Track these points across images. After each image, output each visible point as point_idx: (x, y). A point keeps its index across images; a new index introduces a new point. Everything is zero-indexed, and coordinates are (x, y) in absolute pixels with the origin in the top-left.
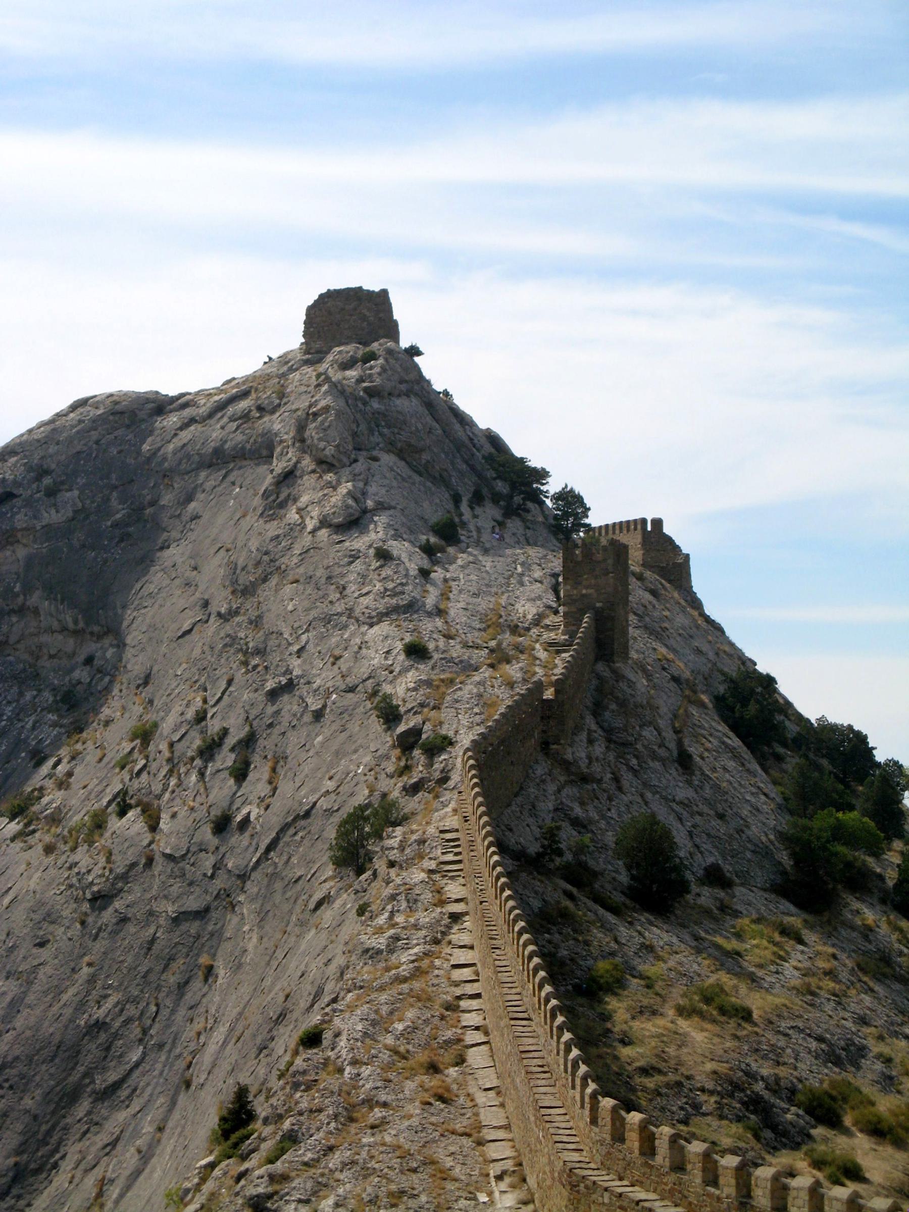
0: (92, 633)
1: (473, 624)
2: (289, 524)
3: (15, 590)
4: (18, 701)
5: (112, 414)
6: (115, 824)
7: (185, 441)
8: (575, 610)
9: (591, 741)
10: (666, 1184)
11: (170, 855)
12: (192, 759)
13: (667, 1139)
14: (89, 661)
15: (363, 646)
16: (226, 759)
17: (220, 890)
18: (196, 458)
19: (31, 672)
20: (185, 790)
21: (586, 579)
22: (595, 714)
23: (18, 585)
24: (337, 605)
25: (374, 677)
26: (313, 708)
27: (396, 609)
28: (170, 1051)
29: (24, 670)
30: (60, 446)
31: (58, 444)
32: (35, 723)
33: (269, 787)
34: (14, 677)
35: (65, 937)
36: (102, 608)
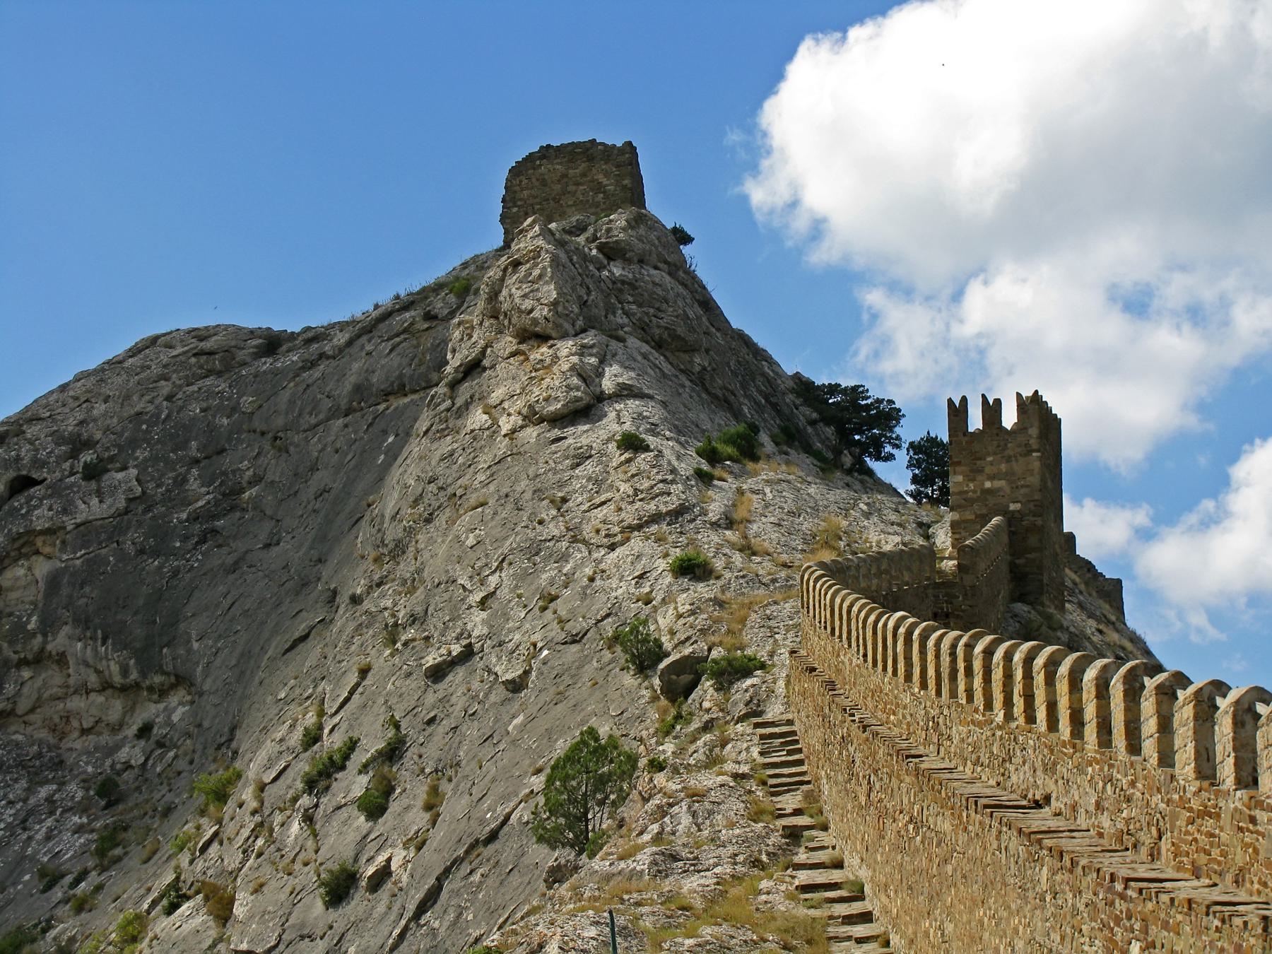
0: (151, 689)
1: (793, 544)
2: (472, 431)
3: (29, 627)
4: (25, 800)
5: (195, 355)
6: (162, 925)
7: (310, 381)
8: (973, 517)
12: (295, 799)
14: (145, 731)
16: (355, 784)
18: (328, 404)
23: (34, 618)
24: (550, 526)
26: (509, 676)
27: (656, 518)
29: (39, 755)
30: (110, 404)
31: (106, 401)
32: (50, 830)
33: (427, 816)
34: (21, 765)
36: (168, 645)
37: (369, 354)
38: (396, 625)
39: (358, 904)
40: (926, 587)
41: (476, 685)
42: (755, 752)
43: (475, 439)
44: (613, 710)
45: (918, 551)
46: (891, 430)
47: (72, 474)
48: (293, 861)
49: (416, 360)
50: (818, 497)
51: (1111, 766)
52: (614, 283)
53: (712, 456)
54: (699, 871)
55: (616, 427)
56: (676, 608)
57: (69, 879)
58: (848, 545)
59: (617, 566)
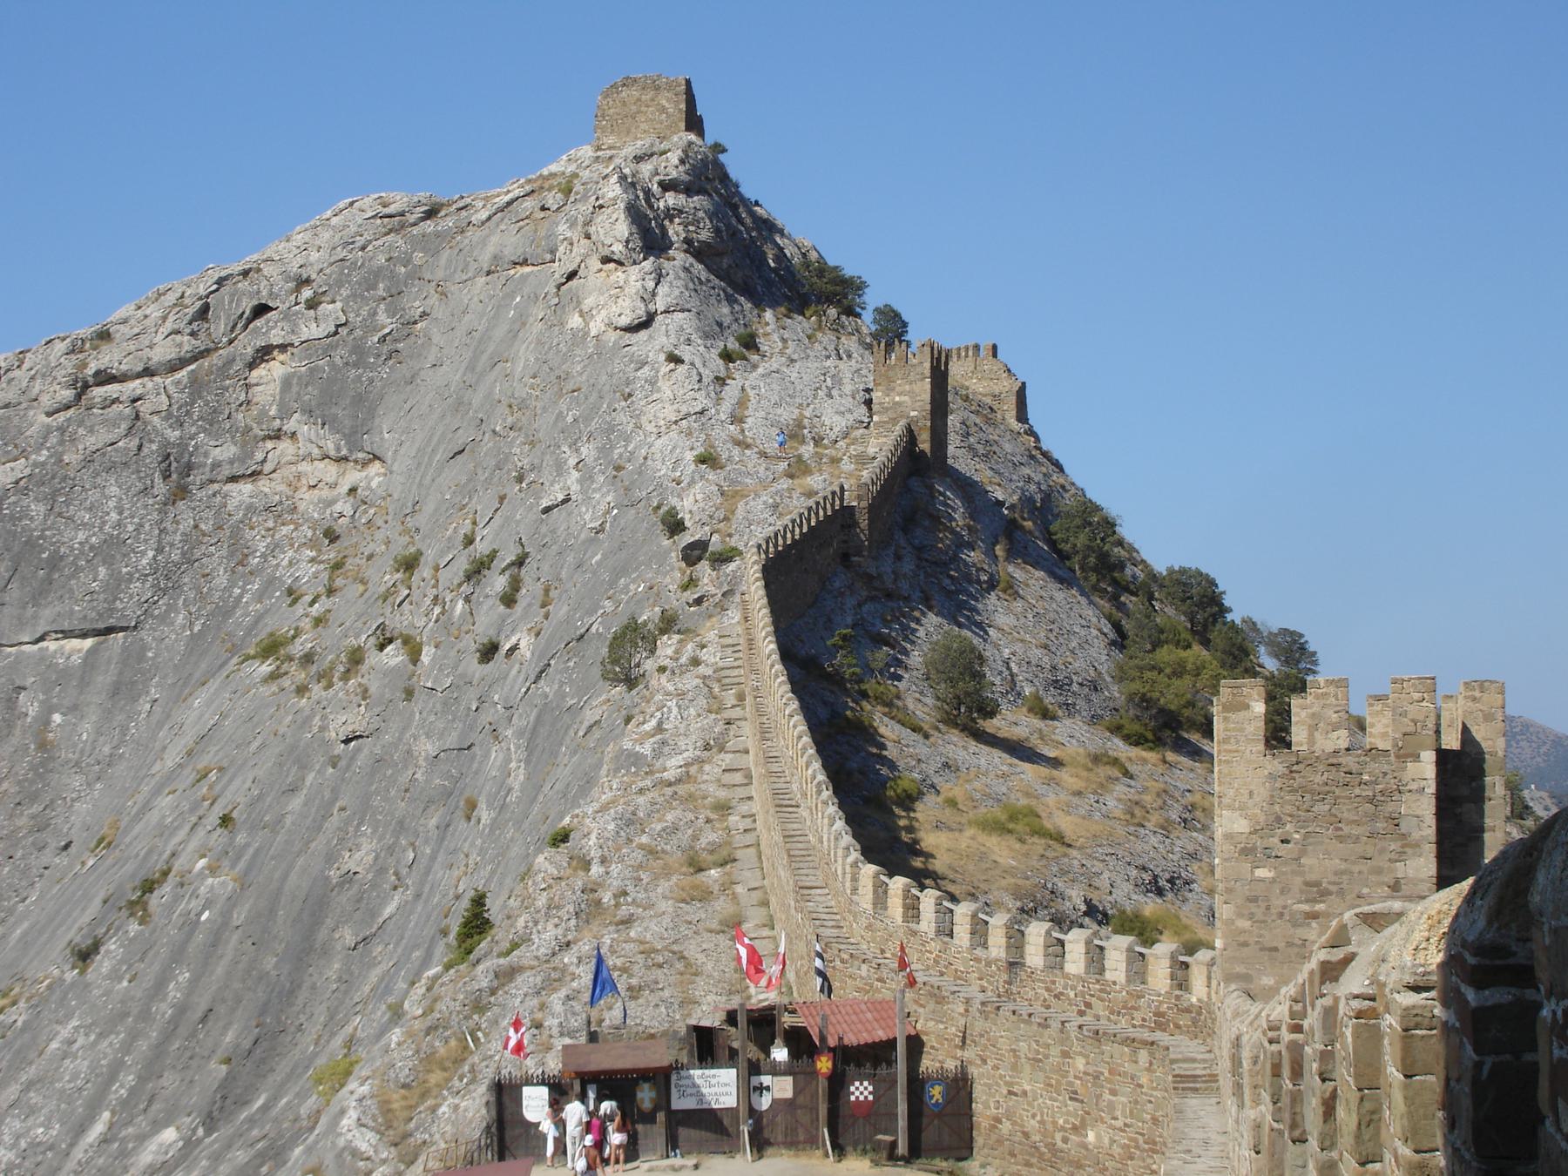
0: (356, 461)
9: (898, 558)
10: (931, 952)
12: (460, 585)
14: (353, 490)
16: (498, 583)
22: (905, 530)
26: (592, 525)
27: (688, 415)
28: (427, 901)
42: (719, 655)
47: (296, 304)
53: (727, 357)
57: (308, 598)
59: (661, 451)
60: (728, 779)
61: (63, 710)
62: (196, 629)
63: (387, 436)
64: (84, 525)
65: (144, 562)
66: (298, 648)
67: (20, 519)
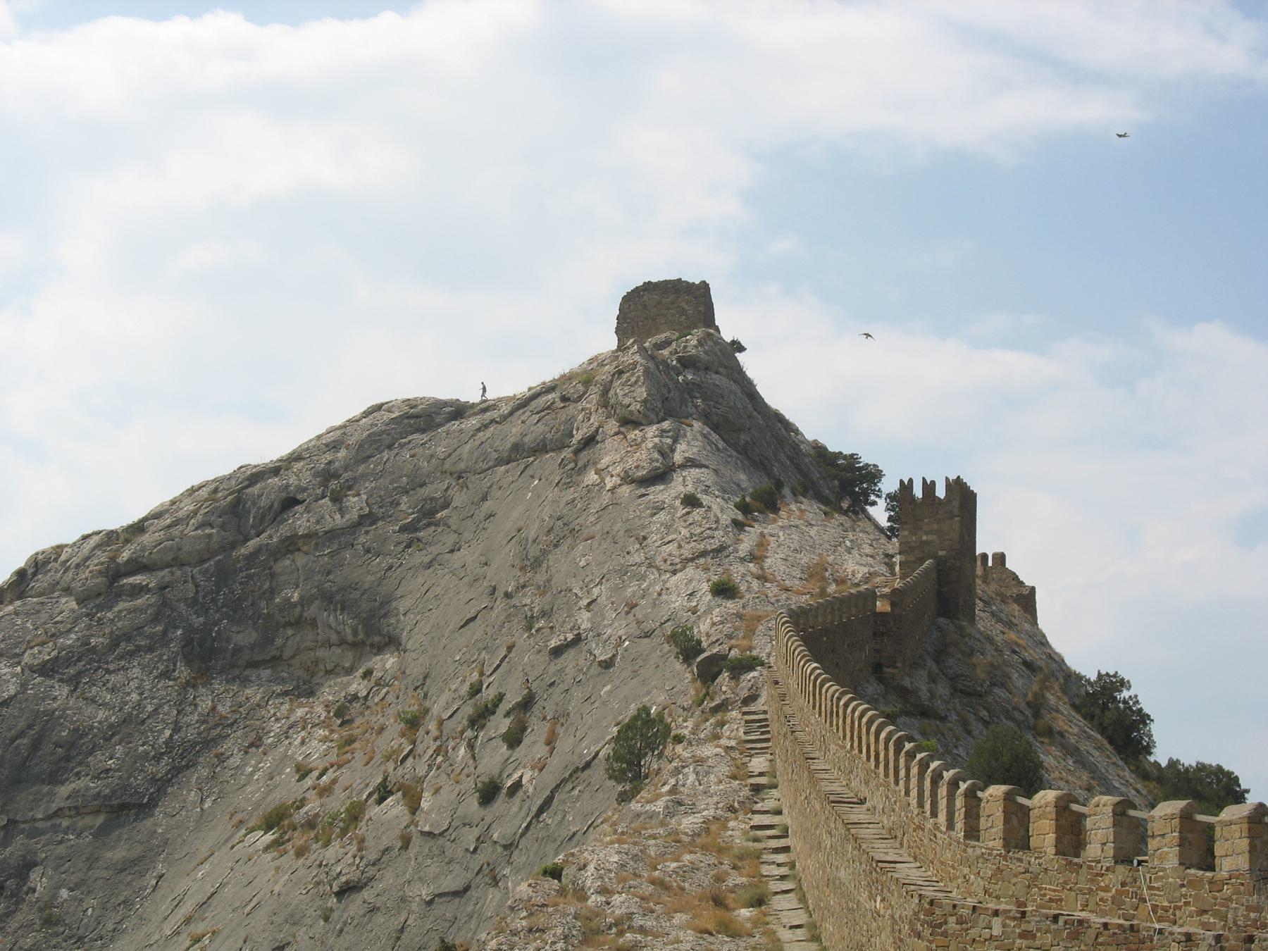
0: (372, 645)
1: (794, 574)
2: (587, 486)
6: (374, 811)
7: (483, 439)
8: (914, 559)
11: (429, 834)
12: (462, 732)
13: (1110, 809)
15: (664, 592)
16: (501, 724)
17: (483, 865)
18: (495, 455)
19: (305, 690)
20: (451, 765)
21: (927, 524)
25: (674, 620)
26: (602, 658)
27: (703, 554)
33: (547, 748)
35: (306, 937)
37: (523, 422)
38: (532, 617)
39: (500, 804)
40: (869, 616)
41: (582, 662)
42: (742, 730)
43: (589, 491)
44: (668, 686)
45: (864, 594)
46: (875, 484)
47: (323, 497)
48: (460, 774)
49: (555, 429)
50: (816, 538)
51: (888, 790)
52: (687, 384)
53: (744, 508)
54: (694, 813)
55: (681, 488)
56: (711, 619)
57: (316, 773)
58: (832, 574)
59: (677, 586)
60: (759, 833)
61: (72, 885)
62: (206, 806)
63: (402, 618)
64: (104, 704)
65: (161, 741)
66: (300, 816)
67: (43, 699)
